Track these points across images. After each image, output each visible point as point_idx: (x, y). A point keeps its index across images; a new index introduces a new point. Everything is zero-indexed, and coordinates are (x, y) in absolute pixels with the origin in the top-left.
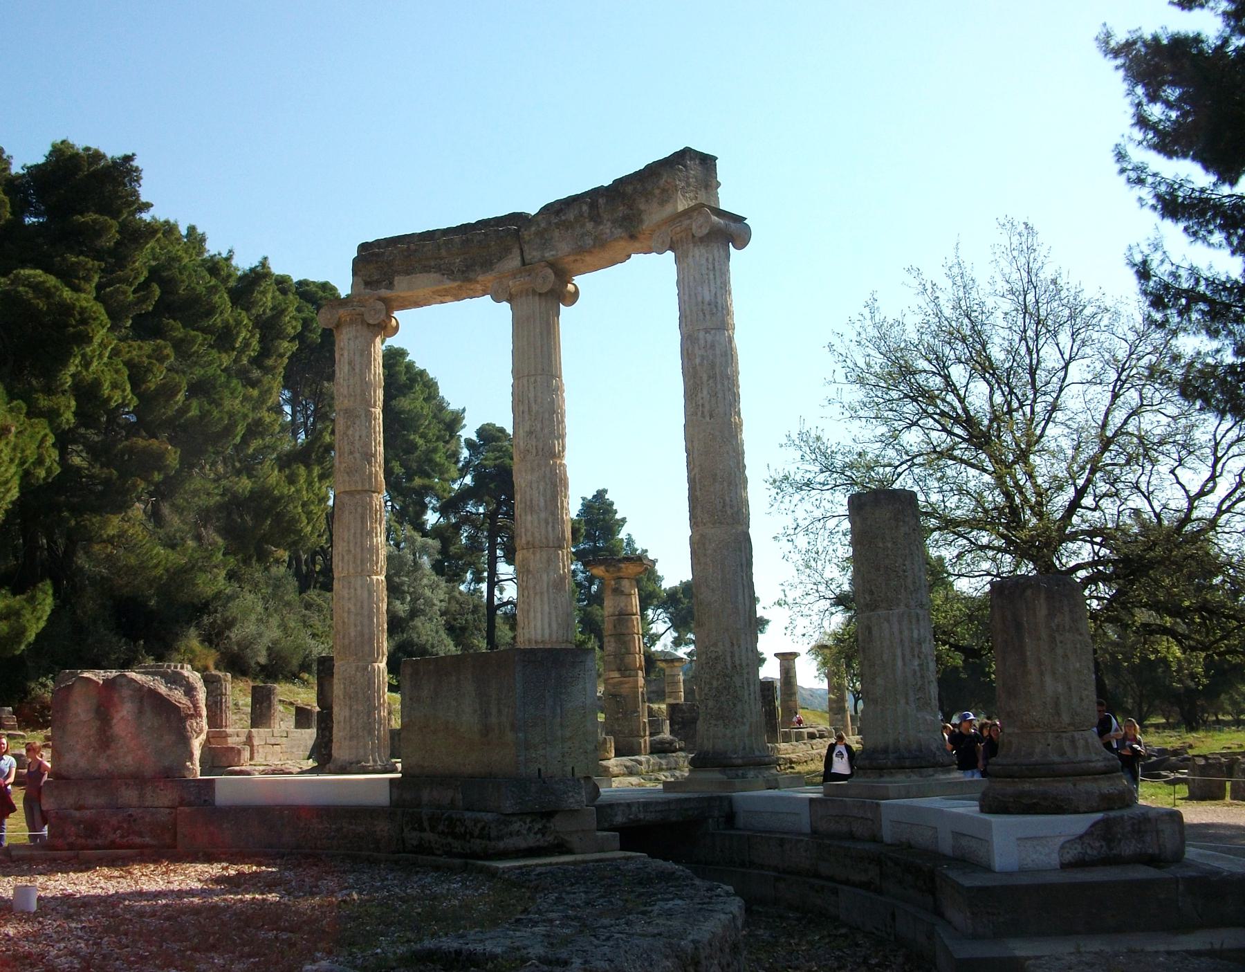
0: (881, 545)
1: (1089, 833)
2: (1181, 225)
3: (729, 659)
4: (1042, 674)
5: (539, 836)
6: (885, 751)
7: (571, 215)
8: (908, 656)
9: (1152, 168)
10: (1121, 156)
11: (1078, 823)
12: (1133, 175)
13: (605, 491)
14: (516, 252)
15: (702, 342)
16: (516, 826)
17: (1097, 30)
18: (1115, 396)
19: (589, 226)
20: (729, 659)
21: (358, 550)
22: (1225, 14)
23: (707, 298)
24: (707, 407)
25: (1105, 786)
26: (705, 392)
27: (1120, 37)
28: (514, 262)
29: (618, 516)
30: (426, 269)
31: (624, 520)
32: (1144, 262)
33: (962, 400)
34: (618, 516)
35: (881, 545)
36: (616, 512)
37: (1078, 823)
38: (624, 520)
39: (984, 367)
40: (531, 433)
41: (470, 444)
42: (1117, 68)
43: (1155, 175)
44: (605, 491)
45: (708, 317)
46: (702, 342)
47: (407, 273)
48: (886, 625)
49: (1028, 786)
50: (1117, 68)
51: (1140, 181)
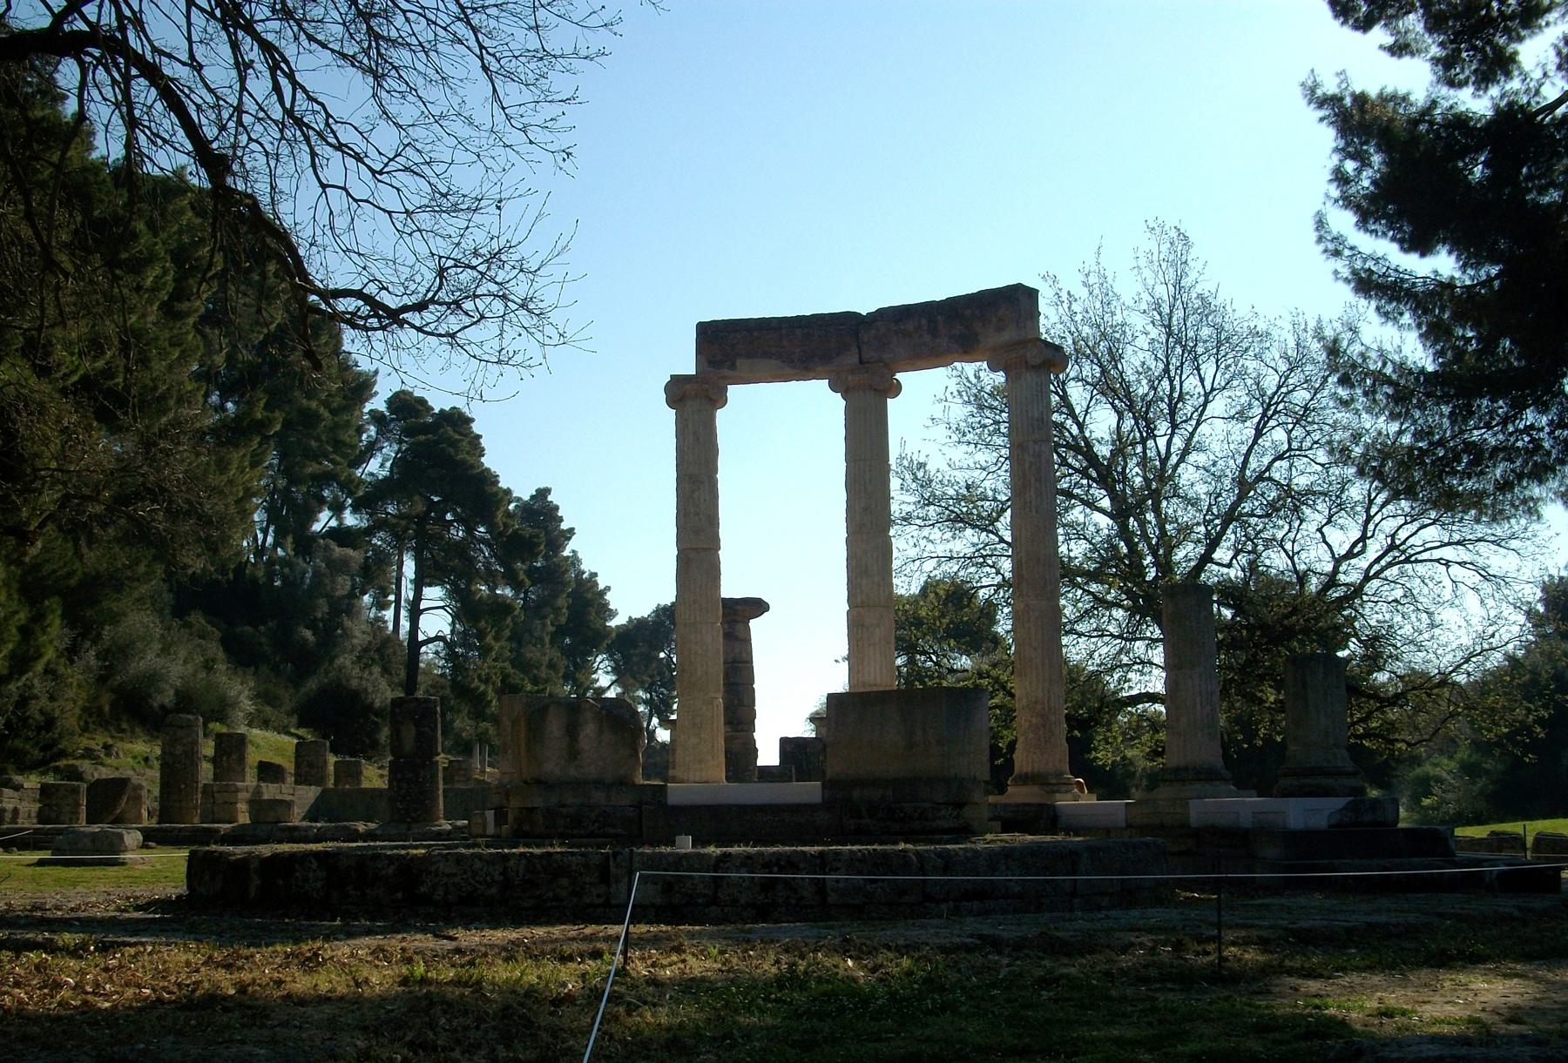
1: (1344, 808)
2: (1374, 304)
6: (1186, 768)
7: (910, 326)
9: (1351, 241)
10: (1320, 223)
11: (1340, 802)
12: (1331, 246)
13: (547, 491)
14: (854, 350)
17: (1303, 75)
18: (1259, 433)
19: (928, 338)
22: (1436, 61)
23: (1036, 415)
25: (1352, 782)
27: (1330, 87)
28: (852, 358)
29: (564, 526)
30: (767, 355)
31: (571, 531)
32: (1335, 341)
33: (1081, 426)
34: (564, 526)
36: (561, 520)
37: (1340, 802)
38: (571, 531)
39: (1111, 387)
40: (866, 509)
41: (377, 417)
42: (1321, 120)
43: (1352, 248)
44: (547, 491)
47: (750, 356)
49: (1309, 781)
50: (1321, 120)
51: (1337, 253)
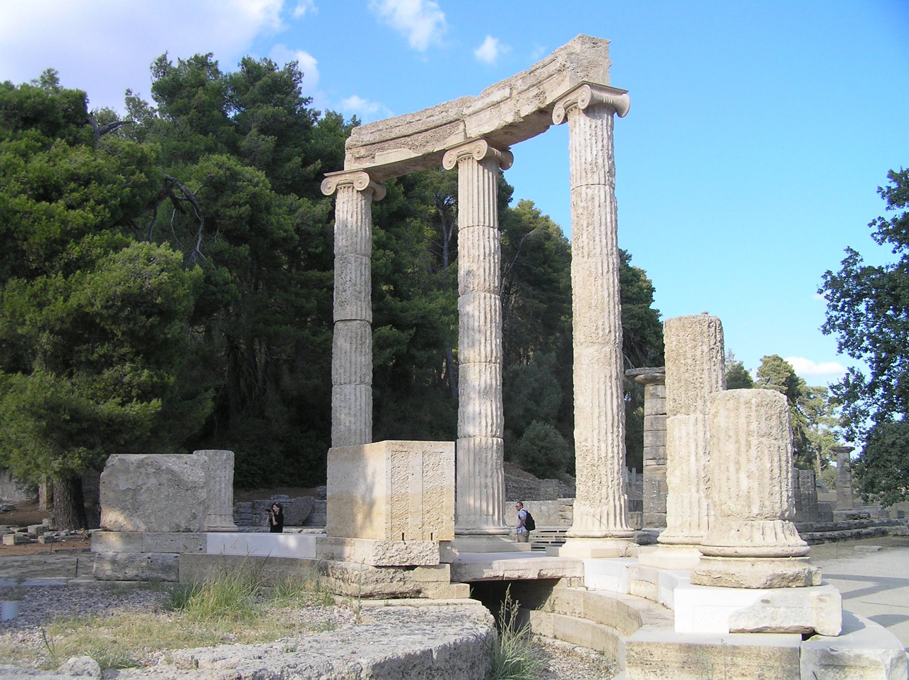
0: (683, 362)
3: (596, 452)
4: (738, 470)
5: (401, 583)
8: (701, 453)
15: (584, 195)
16: (382, 576)
20: (596, 452)
21: (348, 365)
23: (589, 160)
24: (586, 249)
26: (585, 236)
35: (683, 362)
45: (589, 175)
46: (584, 195)
48: (683, 426)
